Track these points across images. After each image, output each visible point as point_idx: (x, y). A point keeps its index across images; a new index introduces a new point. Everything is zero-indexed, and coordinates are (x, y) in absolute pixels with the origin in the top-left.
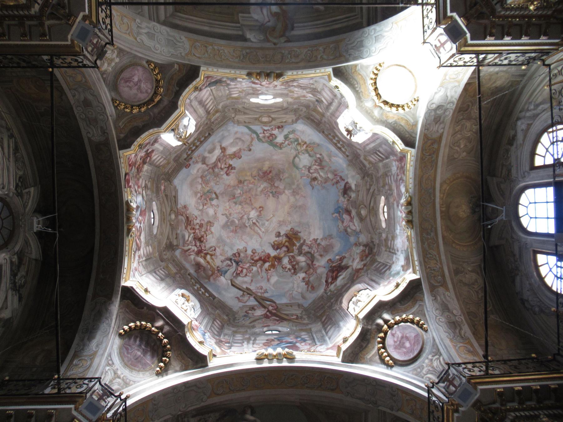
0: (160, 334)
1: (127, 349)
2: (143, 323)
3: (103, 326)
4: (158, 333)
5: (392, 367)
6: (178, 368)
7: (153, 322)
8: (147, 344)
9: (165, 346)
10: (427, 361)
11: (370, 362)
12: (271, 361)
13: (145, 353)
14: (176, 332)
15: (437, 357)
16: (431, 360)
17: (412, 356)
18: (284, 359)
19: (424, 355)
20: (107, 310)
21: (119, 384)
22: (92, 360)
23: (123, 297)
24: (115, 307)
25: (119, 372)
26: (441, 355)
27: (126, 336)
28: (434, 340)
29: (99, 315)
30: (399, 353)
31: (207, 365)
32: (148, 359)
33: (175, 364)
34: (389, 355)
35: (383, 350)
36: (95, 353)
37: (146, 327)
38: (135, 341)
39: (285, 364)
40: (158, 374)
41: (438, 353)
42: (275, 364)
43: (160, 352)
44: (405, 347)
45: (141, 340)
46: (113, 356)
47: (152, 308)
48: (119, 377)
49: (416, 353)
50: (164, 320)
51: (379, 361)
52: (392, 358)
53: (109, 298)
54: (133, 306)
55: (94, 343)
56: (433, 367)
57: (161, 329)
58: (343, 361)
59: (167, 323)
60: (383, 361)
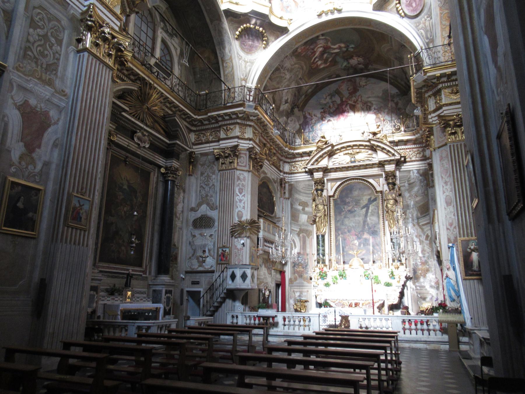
0: (257, 27)
1: (244, 44)
2: (245, 25)
3: (226, 38)
4: (255, 27)
5: (403, 17)
6: (273, 40)
7: (249, 22)
8: (252, 35)
9: (262, 32)
10: (423, 19)
11: (390, 11)
12: (327, 14)
13: (253, 41)
14: (265, 21)
15: (429, 19)
16: (426, 20)
17: (415, 14)
18: (336, 11)
19: (423, 14)
20: (222, 28)
21: (249, 66)
22: (232, 61)
23: (227, 17)
24: (226, 25)
25: (246, 60)
26: (431, 18)
27: (239, 38)
28: (431, 5)
29: (220, 32)
30: (408, 9)
31: (289, 31)
32: (256, 43)
33: (271, 38)
34: (402, 9)
35: (398, 5)
36: (231, 57)
37: (247, 27)
38: (245, 37)
39: (337, 16)
40: (264, 48)
41: (430, 16)
42: (330, 17)
43: (261, 36)
44: (412, 6)
45: (248, 35)
46: (239, 53)
47: (245, 15)
48: (247, 62)
49: (418, 12)
50: (255, 18)
51: (396, 12)
52: (403, 12)
53: (219, 19)
54: (235, 19)
55: (227, 50)
56: (425, 26)
57: (255, 24)
58: (374, 10)
59: (257, 19)
60: (398, 12)
